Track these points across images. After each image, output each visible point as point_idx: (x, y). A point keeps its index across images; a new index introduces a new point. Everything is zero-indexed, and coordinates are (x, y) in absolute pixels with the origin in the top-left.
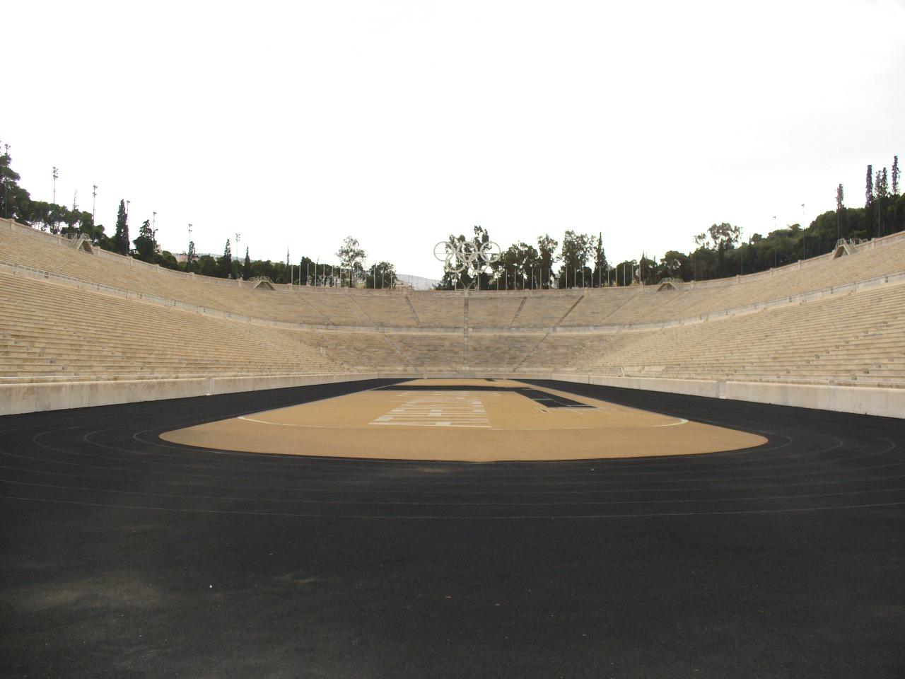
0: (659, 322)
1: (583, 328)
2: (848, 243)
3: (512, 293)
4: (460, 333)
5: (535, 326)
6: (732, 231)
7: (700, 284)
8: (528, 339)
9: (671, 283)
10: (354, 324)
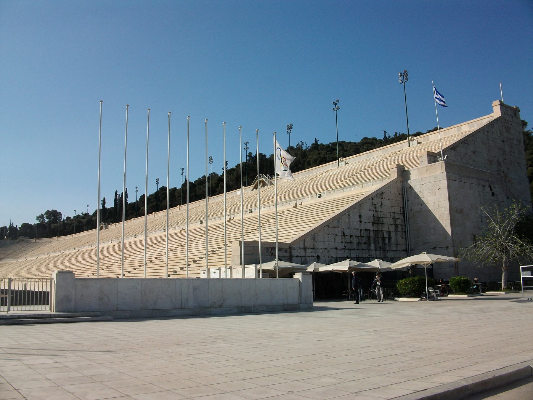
2: (105, 224)
7: (38, 240)
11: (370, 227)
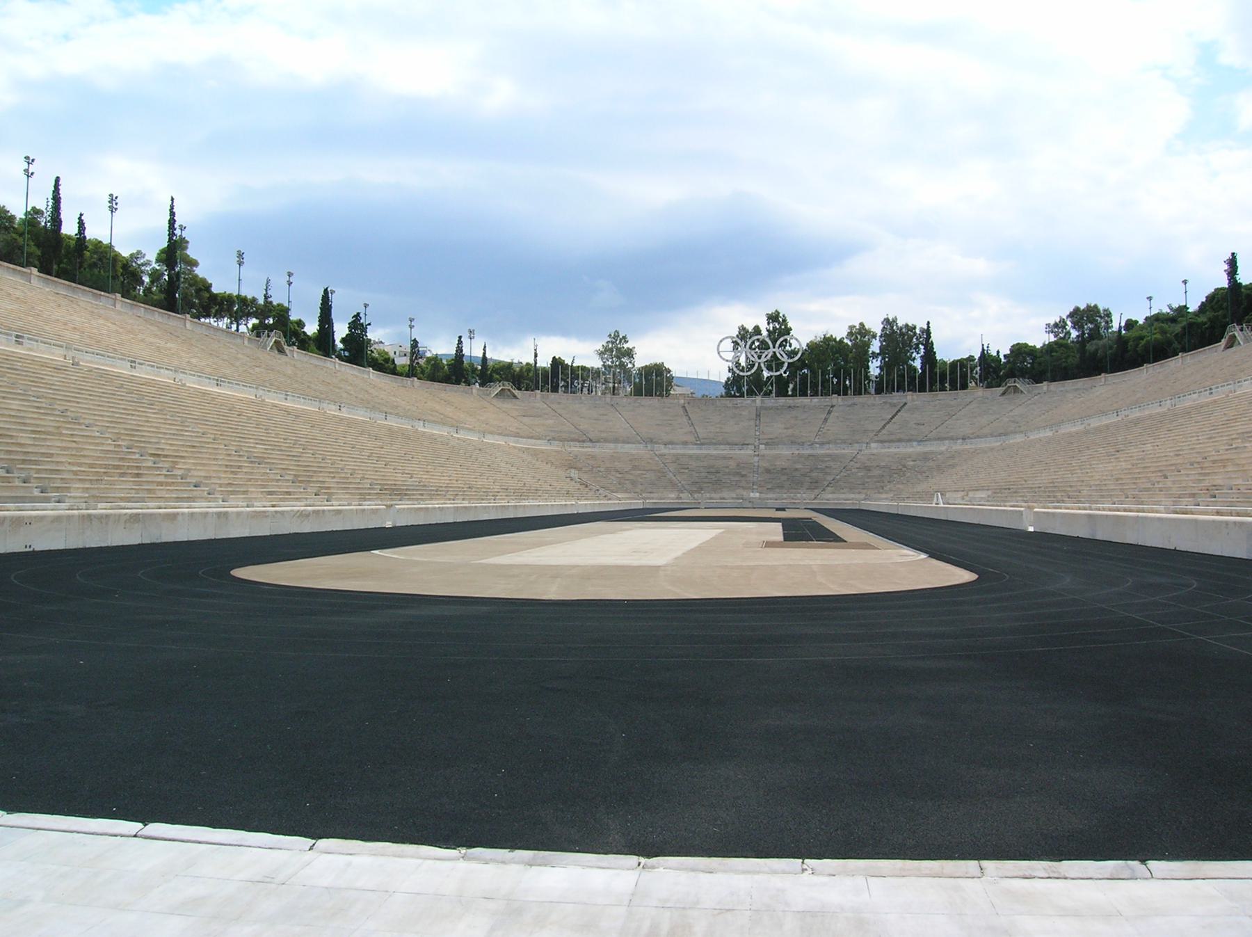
0: (1000, 435)
1: (903, 443)
2: (1242, 330)
3: (816, 400)
4: (749, 451)
5: (844, 442)
6: (1100, 317)
7: (1054, 386)
8: (834, 458)
9: (1017, 385)
10: (616, 441)
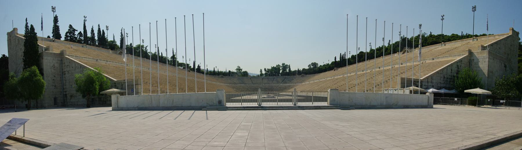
11: (455, 75)
